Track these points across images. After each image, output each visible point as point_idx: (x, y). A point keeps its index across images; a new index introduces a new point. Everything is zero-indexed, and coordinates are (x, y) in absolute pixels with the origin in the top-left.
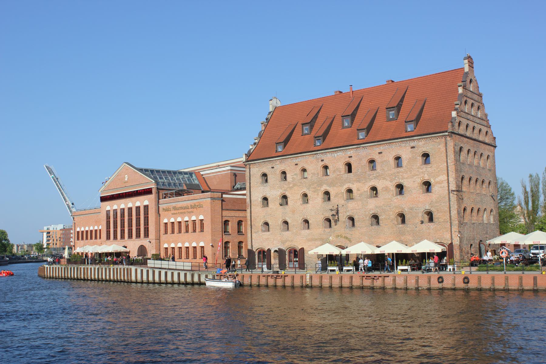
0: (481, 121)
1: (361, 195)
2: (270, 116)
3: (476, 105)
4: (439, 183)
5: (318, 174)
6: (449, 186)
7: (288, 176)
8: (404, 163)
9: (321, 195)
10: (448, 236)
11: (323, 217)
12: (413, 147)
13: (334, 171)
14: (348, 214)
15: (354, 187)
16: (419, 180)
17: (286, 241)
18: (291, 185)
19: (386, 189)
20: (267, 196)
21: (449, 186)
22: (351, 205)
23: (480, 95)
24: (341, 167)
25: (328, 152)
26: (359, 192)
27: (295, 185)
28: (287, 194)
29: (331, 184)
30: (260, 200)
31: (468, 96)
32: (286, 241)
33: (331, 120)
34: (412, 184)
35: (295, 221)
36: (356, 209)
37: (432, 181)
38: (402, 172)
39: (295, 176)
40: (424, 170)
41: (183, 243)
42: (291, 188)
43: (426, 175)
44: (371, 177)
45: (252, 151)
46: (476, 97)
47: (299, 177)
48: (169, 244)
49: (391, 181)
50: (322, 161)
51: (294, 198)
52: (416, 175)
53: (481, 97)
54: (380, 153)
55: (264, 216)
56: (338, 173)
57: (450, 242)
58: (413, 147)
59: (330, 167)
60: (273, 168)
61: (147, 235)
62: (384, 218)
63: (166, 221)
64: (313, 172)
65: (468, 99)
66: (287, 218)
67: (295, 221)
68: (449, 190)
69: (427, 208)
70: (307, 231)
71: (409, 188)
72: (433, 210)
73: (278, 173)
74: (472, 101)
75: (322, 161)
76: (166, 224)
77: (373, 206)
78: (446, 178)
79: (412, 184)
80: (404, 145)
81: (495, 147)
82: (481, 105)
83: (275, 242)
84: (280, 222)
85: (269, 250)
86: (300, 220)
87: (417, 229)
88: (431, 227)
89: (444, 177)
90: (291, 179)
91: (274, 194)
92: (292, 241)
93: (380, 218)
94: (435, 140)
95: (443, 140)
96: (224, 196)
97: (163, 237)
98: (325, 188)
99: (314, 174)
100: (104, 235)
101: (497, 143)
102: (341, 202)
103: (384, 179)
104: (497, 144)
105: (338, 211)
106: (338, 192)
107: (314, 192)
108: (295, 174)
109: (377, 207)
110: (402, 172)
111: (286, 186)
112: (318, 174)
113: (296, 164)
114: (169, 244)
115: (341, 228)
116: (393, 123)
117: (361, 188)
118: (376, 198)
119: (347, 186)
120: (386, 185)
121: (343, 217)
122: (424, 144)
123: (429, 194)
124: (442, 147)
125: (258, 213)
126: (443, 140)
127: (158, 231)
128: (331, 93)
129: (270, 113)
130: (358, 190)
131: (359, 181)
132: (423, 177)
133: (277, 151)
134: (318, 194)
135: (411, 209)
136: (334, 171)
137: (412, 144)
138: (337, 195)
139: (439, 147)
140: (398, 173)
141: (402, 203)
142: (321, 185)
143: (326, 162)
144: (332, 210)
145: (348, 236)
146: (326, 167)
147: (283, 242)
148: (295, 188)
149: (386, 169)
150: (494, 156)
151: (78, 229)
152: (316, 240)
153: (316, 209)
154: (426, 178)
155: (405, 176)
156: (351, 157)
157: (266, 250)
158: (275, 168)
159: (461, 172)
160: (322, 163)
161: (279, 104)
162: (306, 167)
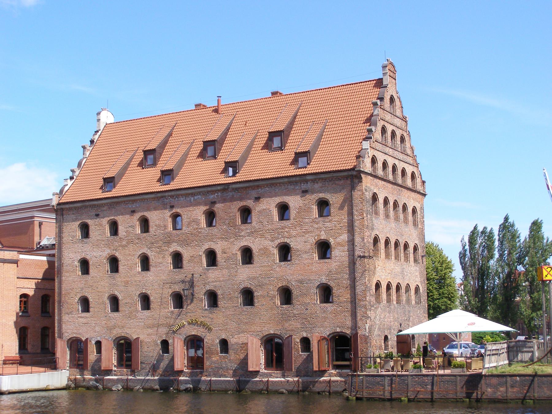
0: (405, 157)
2: (96, 137)
3: (398, 133)
7: (120, 228)
8: (293, 213)
9: (170, 260)
11: (171, 291)
13: (189, 224)
14: (208, 288)
15: (218, 247)
16: (312, 240)
17: (114, 327)
18: (124, 243)
19: (265, 251)
20: (88, 257)
22: (214, 274)
23: (404, 119)
25: (182, 195)
26: (225, 255)
27: (130, 242)
29: (185, 243)
31: (387, 119)
32: (114, 327)
34: (303, 244)
36: (220, 281)
37: (332, 241)
38: (289, 228)
43: (323, 233)
44: (243, 234)
45: (66, 188)
46: (398, 122)
51: (129, 261)
53: (406, 122)
55: (82, 289)
56: (195, 226)
59: (184, 217)
62: (261, 295)
64: (157, 223)
65: (387, 125)
69: (324, 281)
70: (146, 313)
71: (298, 251)
72: (331, 284)
74: (395, 128)
77: (245, 275)
79: (303, 244)
80: (292, 187)
81: (424, 195)
82: (405, 134)
83: (97, 329)
87: (309, 311)
88: (329, 309)
90: (124, 233)
91: (98, 255)
93: (255, 294)
94: (337, 182)
95: (349, 182)
96: (22, 256)
99: (158, 226)
101: (428, 189)
103: (262, 236)
104: (427, 191)
106: (193, 254)
107: (159, 253)
109: (249, 278)
110: (289, 228)
115: (198, 308)
116: (278, 155)
117: (228, 248)
118: (249, 265)
119: (206, 246)
120: (264, 245)
121: (200, 292)
122: (321, 187)
123: (326, 260)
125: (72, 284)
126: (349, 182)
129: (97, 132)
131: (226, 239)
134: (164, 257)
135: (301, 282)
136: (189, 224)
137: (304, 187)
141: (289, 274)
142: (169, 243)
144: (183, 282)
145: (207, 321)
150: (422, 208)
152: (158, 326)
153: (160, 280)
154: (323, 237)
155: (294, 233)
157: (84, 339)
159: (373, 229)
161: (111, 120)
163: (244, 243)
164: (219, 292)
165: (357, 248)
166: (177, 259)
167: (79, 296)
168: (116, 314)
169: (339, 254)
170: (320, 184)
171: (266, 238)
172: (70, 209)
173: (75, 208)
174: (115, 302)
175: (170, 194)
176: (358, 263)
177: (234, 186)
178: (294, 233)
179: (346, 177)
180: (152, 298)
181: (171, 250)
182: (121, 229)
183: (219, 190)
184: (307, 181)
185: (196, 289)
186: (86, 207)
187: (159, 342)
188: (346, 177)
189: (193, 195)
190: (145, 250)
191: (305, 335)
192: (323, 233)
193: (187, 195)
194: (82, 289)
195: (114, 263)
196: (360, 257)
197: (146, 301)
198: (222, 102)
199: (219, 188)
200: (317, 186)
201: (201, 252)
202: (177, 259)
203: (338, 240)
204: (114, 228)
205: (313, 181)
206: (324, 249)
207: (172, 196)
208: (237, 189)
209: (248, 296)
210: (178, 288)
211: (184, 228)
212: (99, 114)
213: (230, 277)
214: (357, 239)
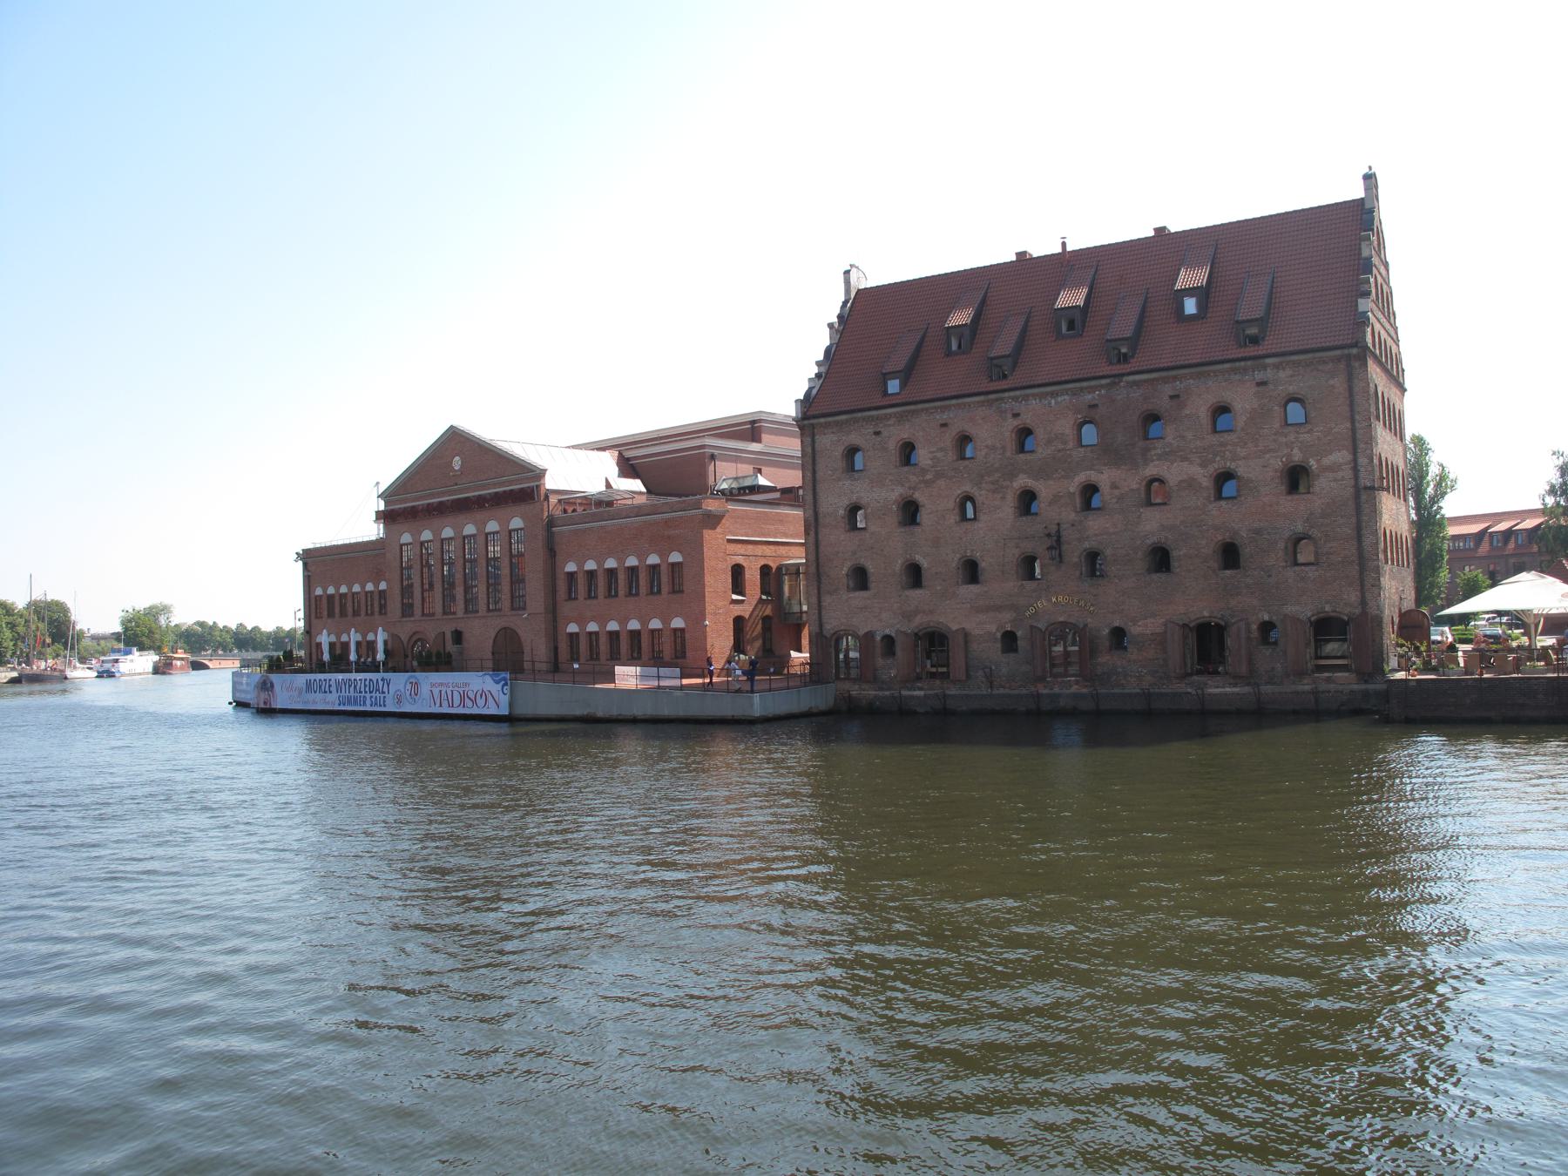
1: (1120, 498)
4: (1332, 468)
5: (1004, 448)
6: (1356, 478)
8: (1241, 422)
10: (1353, 596)
11: (1017, 552)
12: (1259, 384)
13: (1049, 442)
14: (1087, 545)
15: (1104, 477)
16: (1277, 464)
18: (928, 477)
19: (1190, 484)
21: (1356, 478)
22: (1095, 523)
24: (1067, 431)
25: (1034, 395)
26: (1117, 492)
28: (919, 496)
30: (841, 512)
33: (1022, 319)
34: (1260, 470)
35: (939, 561)
37: (1312, 462)
39: (939, 455)
40: (1292, 437)
41: (623, 621)
42: (928, 483)
43: (1296, 451)
47: (951, 455)
48: (582, 622)
49: (1203, 465)
50: (1016, 415)
51: (937, 505)
52: (1270, 451)
54: (1172, 397)
56: (1061, 446)
57: (1357, 611)
58: (1259, 384)
59: (1040, 433)
60: (877, 433)
61: (518, 604)
63: (571, 567)
64: (989, 442)
66: (918, 557)
67: (939, 561)
68: (1356, 486)
70: (973, 588)
73: (893, 445)
75: (1016, 415)
76: (571, 575)
77: (1152, 525)
78: (1349, 457)
79: (1260, 470)
80: (1237, 377)
84: (899, 565)
85: (870, 635)
86: (954, 560)
89: (1341, 456)
92: (932, 612)
93: (1174, 554)
97: (566, 608)
98: (1022, 481)
99: (992, 448)
100: (394, 606)
102: (1069, 515)
105: (1059, 537)
108: (941, 449)
111: (913, 478)
112: (1004, 448)
113: (944, 425)
114: (582, 622)
119: (1082, 477)
124: (1338, 383)
126: (1342, 366)
127: (552, 591)
128: (1011, 257)
130: (1114, 486)
132: (1289, 456)
133: (885, 393)
134: (1003, 498)
135: (1258, 532)
136: (1049, 442)
137: (1259, 376)
138: (1055, 499)
139: (1331, 382)
140: (1222, 445)
141: (1233, 519)
142: (1012, 476)
143: (1027, 419)
146: (1025, 433)
147: (908, 616)
148: (942, 483)
149: (1189, 435)
151: (319, 591)
152: (998, 609)
154: (1297, 456)
155: (1242, 452)
156: (1094, 406)
158: (885, 433)
160: (1016, 422)
162: (970, 430)
163: (1151, 470)
164: (1108, 552)
165: (1362, 475)
166: (1027, 499)
167: (848, 564)
168: (918, 592)
169: (1328, 486)
170: (1289, 372)
171: (1191, 463)
172: (827, 425)
173: (837, 423)
174: (915, 575)
175: (1012, 394)
176: (1364, 497)
177: (1131, 378)
178: (1242, 452)
179: (1339, 359)
180: (983, 565)
181: (1016, 485)
182: (922, 456)
183: (1102, 386)
184: (1265, 367)
185: (1064, 547)
186: (856, 421)
187: (999, 635)
188: (1339, 359)
189: (1052, 394)
190: (968, 488)
191: (1266, 618)
192: (1296, 451)
193: (1042, 396)
194: (854, 553)
195: (910, 512)
196: (1366, 488)
197: (971, 571)
198: (1069, 249)
199: (1104, 382)
200: (1282, 374)
201: (1074, 485)
202: (1027, 499)
203: (1326, 461)
204: (907, 451)
205: (1277, 367)
206: (1296, 478)
207: (1015, 399)
208: (1136, 383)
209: (1161, 559)
210: (1029, 547)
211: (1040, 450)
212: (847, 273)
213: (1121, 529)
214: (1362, 461)
